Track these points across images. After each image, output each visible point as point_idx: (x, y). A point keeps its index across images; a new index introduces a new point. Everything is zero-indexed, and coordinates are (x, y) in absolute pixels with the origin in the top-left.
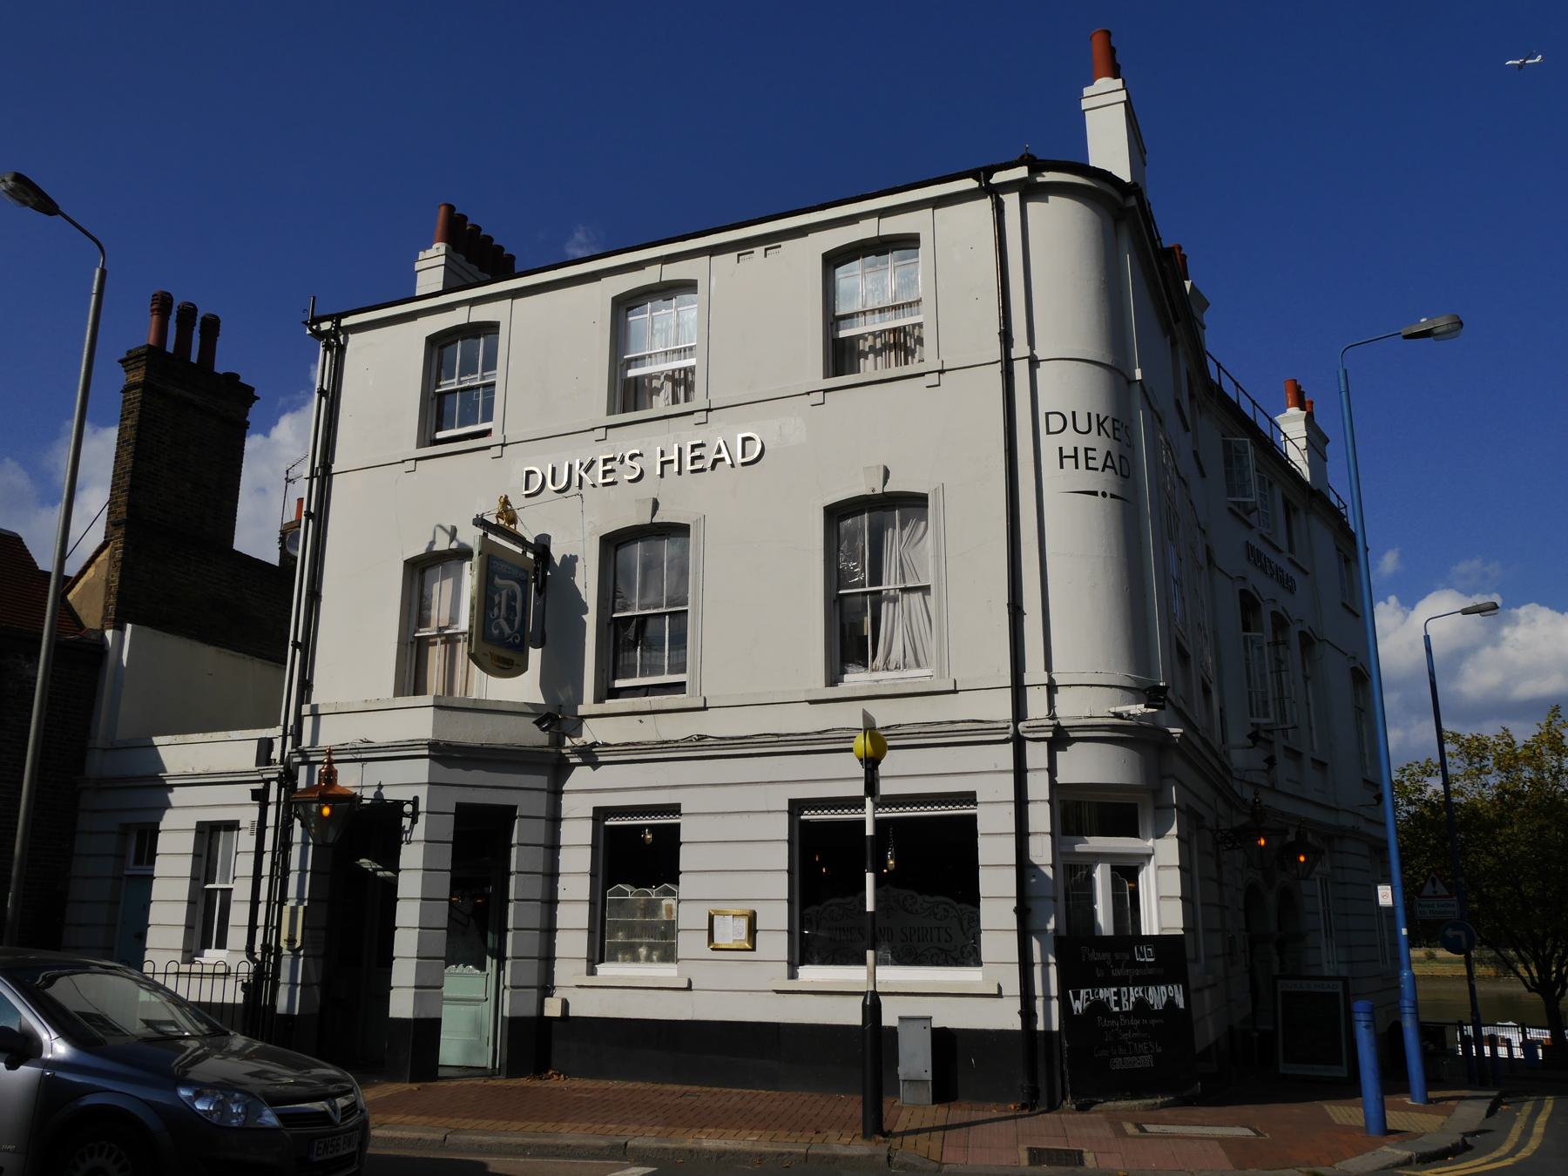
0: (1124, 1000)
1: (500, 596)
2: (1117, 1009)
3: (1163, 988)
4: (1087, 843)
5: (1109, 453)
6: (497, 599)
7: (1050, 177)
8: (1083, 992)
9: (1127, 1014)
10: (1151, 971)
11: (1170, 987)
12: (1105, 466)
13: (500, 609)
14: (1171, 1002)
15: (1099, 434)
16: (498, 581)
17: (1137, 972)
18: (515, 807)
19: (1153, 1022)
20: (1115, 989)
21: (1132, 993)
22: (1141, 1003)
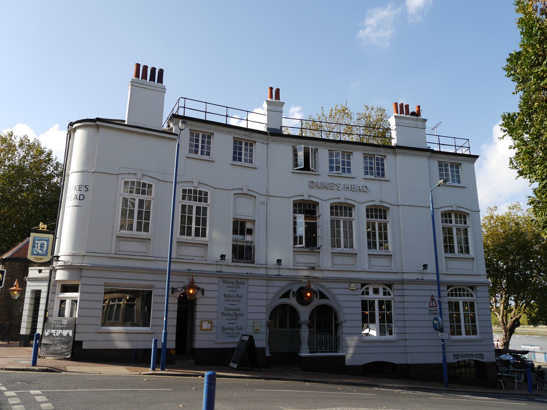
0: (57, 333)
1: (38, 245)
2: (55, 335)
3: (67, 331)
4: (65, 294)
5: (76, 195)
6: (36, 246)
7: (75, 126)
8: (48, 330)
9: (57, 336)
10: (65, 326)
11: (69, 331)
12: (74, 199)
13: (37, 248)
14: (68, 334)
15: (74, 191)
16: (36, 242)
17: (62, 326)
18: (41, 290)
19: (63, 339)
20: (56, 330)
21: (59, 331)
22: (61, 334)
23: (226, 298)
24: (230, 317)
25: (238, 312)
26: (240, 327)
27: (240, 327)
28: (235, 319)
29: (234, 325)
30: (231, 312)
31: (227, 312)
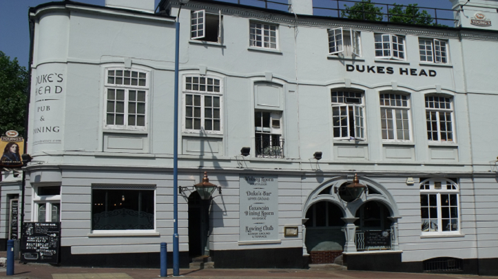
23: (251, 196)
24: (256, 216)
25: (265, 211)
26: (269, 226)
27: (269, 226)
28: (262, 219)
29: (262, 225)
30: (257, 211)
31: (252, 211)
